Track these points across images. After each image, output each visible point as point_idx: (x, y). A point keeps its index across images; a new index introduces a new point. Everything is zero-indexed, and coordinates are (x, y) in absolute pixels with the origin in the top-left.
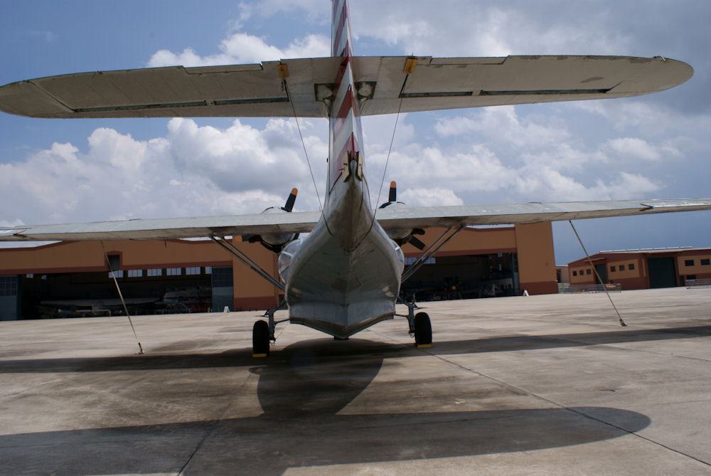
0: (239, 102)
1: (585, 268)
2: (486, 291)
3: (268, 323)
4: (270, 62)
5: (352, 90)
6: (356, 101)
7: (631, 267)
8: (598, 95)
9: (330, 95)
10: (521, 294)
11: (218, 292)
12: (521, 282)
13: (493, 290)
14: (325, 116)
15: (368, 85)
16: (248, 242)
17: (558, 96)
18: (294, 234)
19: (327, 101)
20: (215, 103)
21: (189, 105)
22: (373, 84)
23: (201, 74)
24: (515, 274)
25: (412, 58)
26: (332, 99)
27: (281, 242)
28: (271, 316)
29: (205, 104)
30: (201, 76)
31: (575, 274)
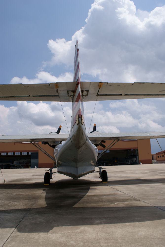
1: (162, 155)
2: (127, 163)
4: (52, 83)
5: (80, 93)
6: (82, 97)
9: (73, 94)
10: (139, 164)
11: (33, 161)
12: (139, 159)
13: (130, 162)
15: (86, 91)
16: (44, 144)
17: (151, 96)
18: (60, 142)
19: (72, 97)
20: (33, 96)
21: (24, 97)
22: (88, 91)
23: (28, 86)
24: (137, 157)
25: (101, 82)
26: (74, 96)
27: (55, 144)
29: (29, 96)
31: (158, 157)
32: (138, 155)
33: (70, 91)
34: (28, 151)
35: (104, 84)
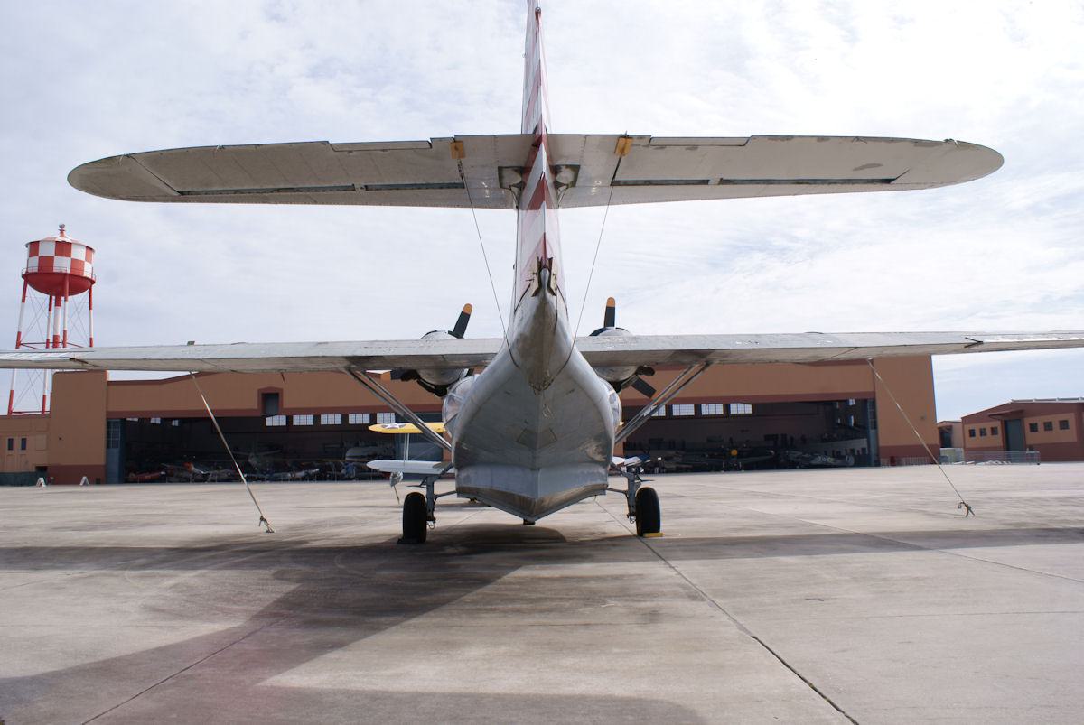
0: (398, 187)
1: (988, 426)
4: (441, 139)
5: (546, 178)
6: (551, 191)
7: (1064, 425)
8: (878, 186)
9: (519, 181)
12: (881, 444)
14: (512, 207)
17: (825, 187)
19: (515, 189)
21: (331, 189)
22: (576, 169)
23: (351, 152)
25: (626, 137)
26: (522, 186)
27: (447, 381)
29: (353, 188)
30: (351, 154)
31: (972, 433)
32: (875, 427)
33: (510, 169)
34: (346, 408)
35: (636, 142)
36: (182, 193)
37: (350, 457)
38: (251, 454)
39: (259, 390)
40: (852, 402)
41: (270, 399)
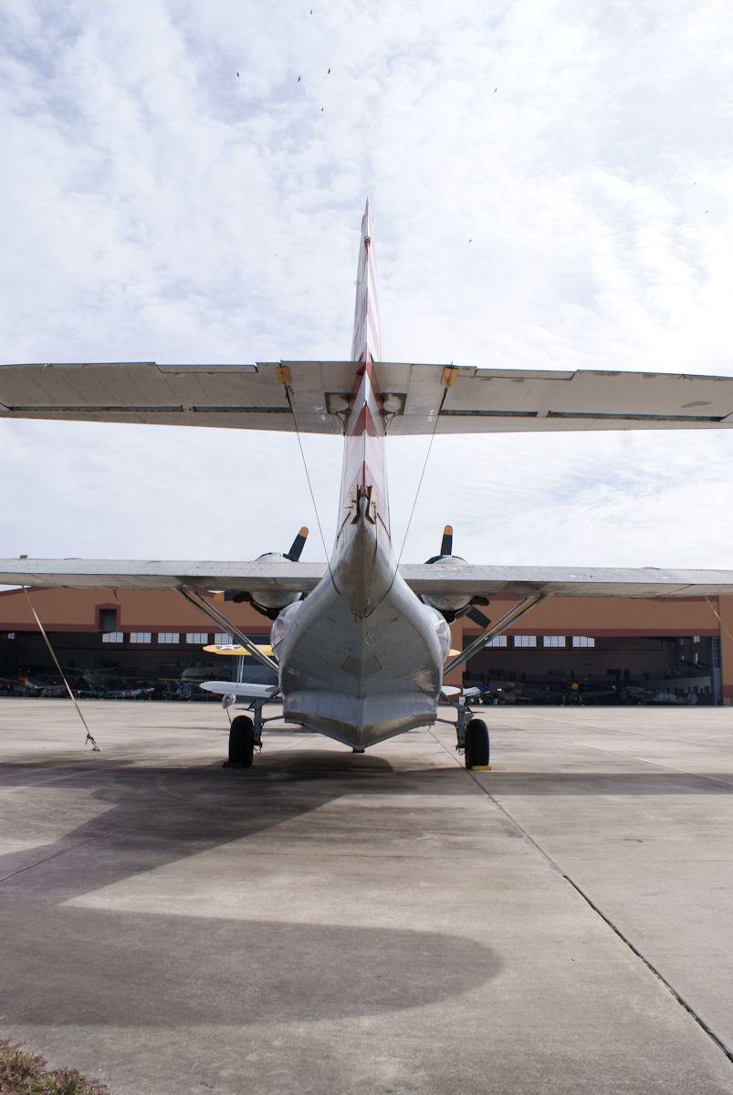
0: (226, 410)
3: (253, 719)
4: (267, 364)
6: (376, 420)
8: (708, 423)
14: (340, 433)
15: (396, 399)
16: (232, 602)
17: (654, 422)
18: (300, 594)
19: (343, 416)
20: (195, 409)
22: (403, 397)
23: (178, 373)
26: (348, 413)
28: (258, 712)
29: (181, 409)
30: (178, 376)
33: (336, 396)
35: (461, 372)
36: (12, 409)
37: (186, 677)
38: (87, 670)
39: (97, 606)
40: (697, 639)
41: (108, 615)
